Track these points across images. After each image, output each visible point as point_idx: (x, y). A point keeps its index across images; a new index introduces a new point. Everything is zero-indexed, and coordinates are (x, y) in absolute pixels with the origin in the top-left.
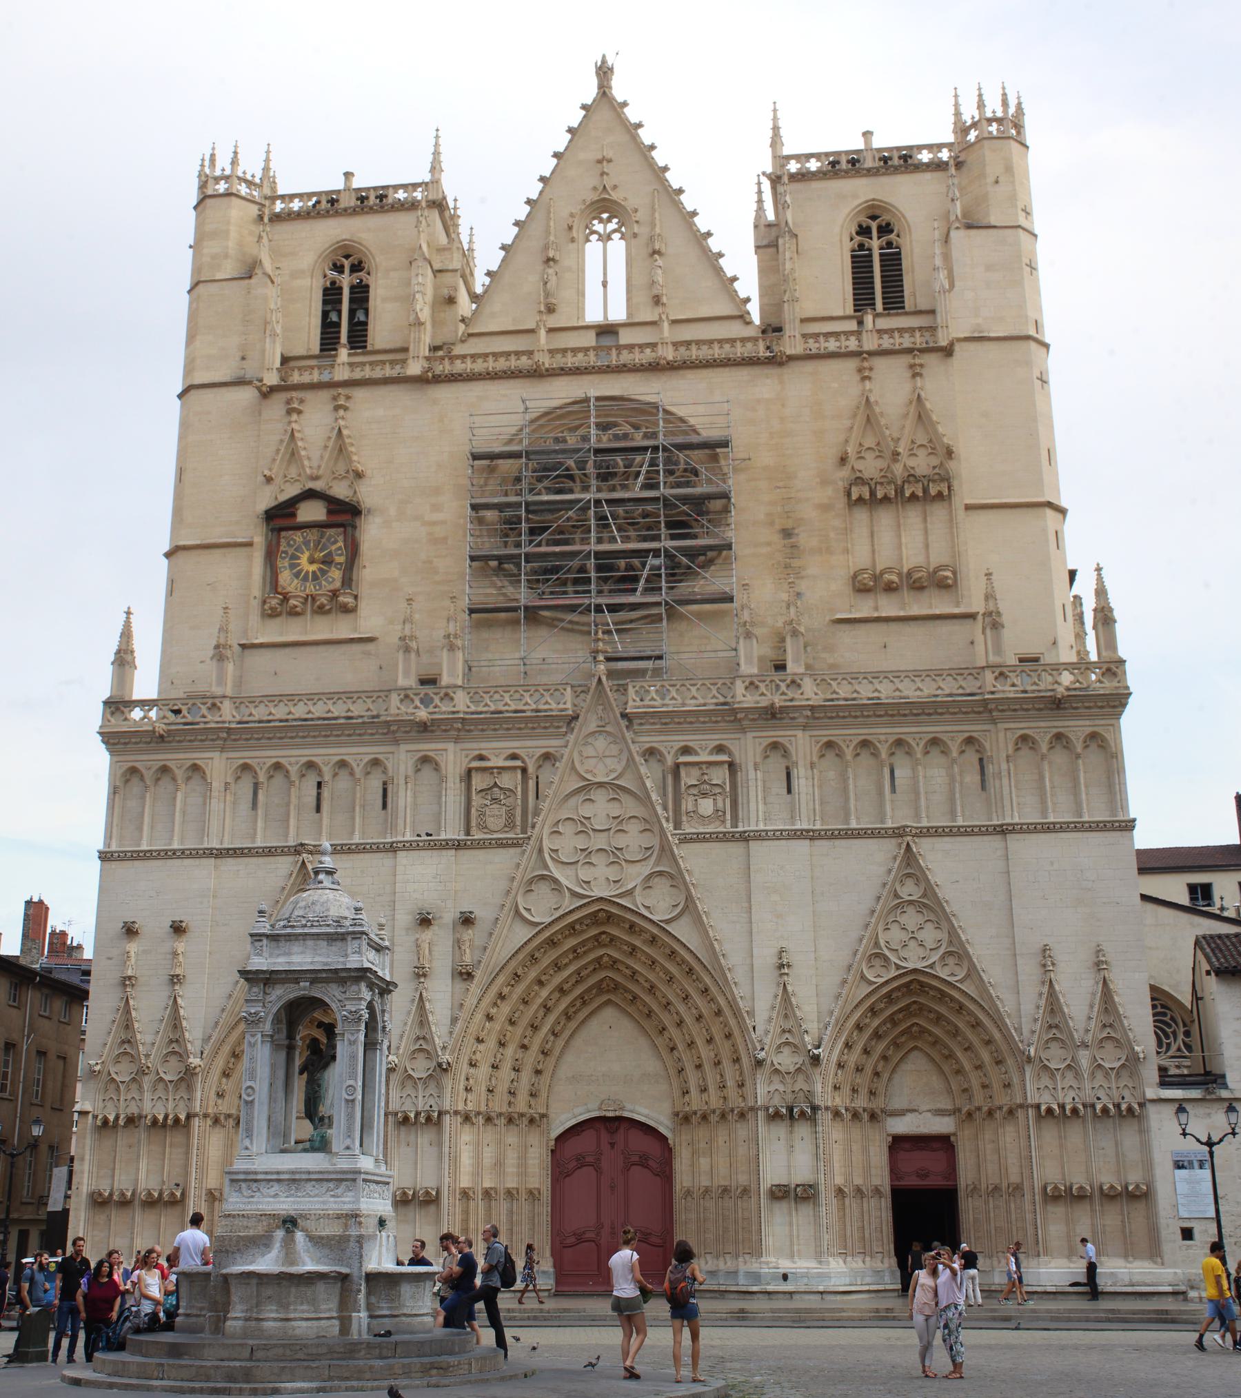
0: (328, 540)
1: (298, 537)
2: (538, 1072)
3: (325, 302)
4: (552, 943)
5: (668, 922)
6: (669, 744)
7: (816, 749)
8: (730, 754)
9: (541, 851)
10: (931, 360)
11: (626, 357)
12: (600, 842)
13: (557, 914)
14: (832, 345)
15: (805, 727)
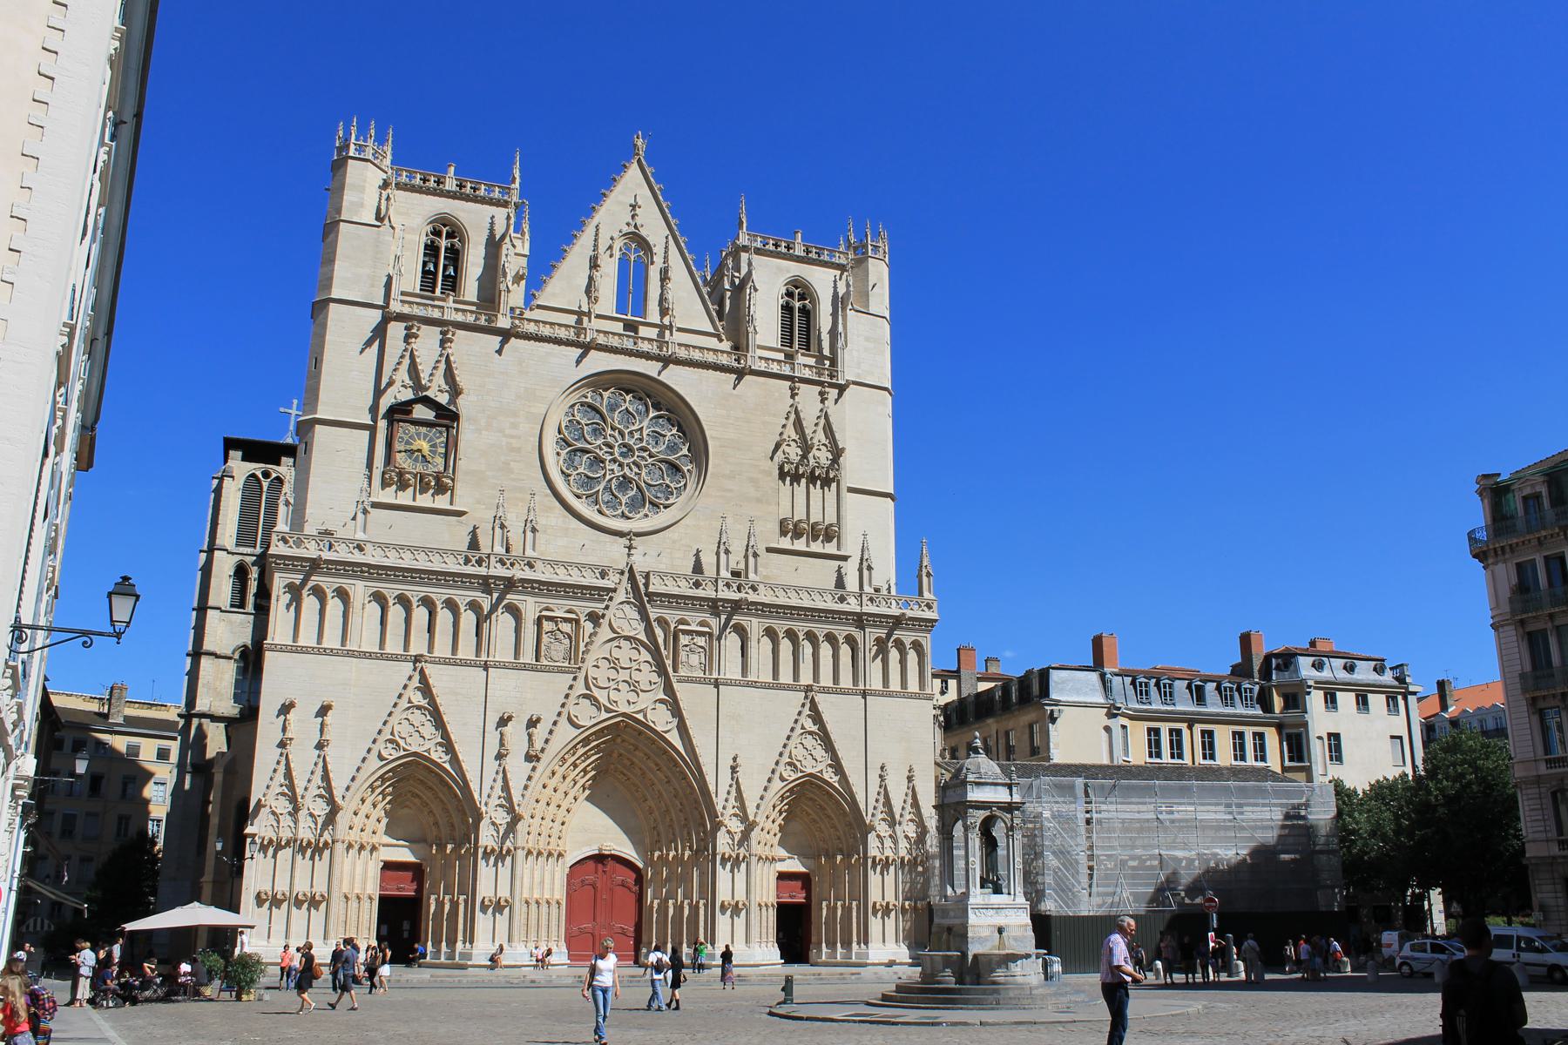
0: (434, 434)
1: (412, 429)
2: (563, 824)
3: (425, 254)
4: (586, 741)
5: (666, 732)
6: (672, 616)
7: (761, 631)
8: (710, 627)
9: (586, 678)
10: (834, 393)
11: (645, 347)
12: (624, 675)
13: (594, 721)
14: (775, 368)
15: (758, 616)
